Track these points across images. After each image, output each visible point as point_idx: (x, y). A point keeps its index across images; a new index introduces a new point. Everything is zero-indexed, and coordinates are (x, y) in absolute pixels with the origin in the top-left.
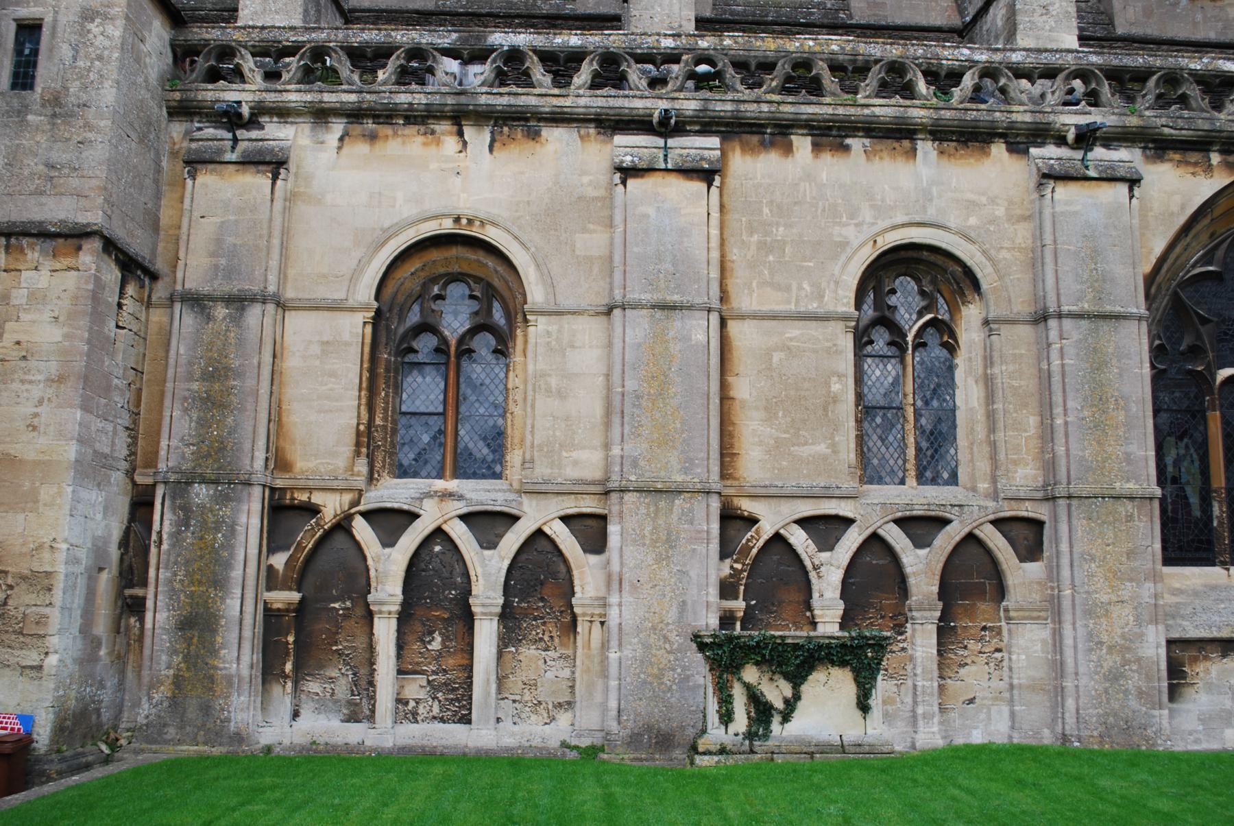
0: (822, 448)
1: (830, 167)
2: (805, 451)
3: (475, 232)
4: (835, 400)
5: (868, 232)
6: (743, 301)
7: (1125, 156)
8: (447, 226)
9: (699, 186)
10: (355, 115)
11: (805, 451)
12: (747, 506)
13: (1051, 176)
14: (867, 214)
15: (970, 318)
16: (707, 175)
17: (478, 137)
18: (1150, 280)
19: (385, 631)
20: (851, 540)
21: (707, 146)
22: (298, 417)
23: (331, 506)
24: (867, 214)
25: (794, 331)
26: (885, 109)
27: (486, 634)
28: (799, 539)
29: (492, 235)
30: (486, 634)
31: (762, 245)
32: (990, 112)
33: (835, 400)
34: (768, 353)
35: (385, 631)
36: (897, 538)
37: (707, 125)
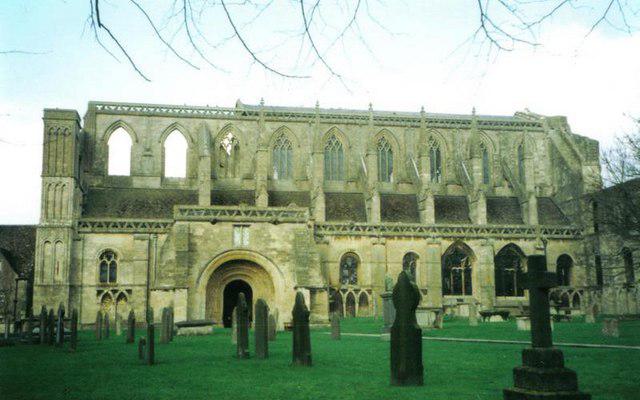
1: (399, 242)
6: (389, 260)
7: (439, 239)
10: (336, 235)
13: (429, 244)
15: (418, 262)
16: (384, 244)
17: (353, 238)
18: (442, 257)
19: (344, 305)
21: (383, 240)
22: (332, 277)
23: (336, 289)
26: (407, 233)
27: (357, 305)
30: (357, 305)
32: (420, 234)
35: (344, 305)
37: (384, 236)
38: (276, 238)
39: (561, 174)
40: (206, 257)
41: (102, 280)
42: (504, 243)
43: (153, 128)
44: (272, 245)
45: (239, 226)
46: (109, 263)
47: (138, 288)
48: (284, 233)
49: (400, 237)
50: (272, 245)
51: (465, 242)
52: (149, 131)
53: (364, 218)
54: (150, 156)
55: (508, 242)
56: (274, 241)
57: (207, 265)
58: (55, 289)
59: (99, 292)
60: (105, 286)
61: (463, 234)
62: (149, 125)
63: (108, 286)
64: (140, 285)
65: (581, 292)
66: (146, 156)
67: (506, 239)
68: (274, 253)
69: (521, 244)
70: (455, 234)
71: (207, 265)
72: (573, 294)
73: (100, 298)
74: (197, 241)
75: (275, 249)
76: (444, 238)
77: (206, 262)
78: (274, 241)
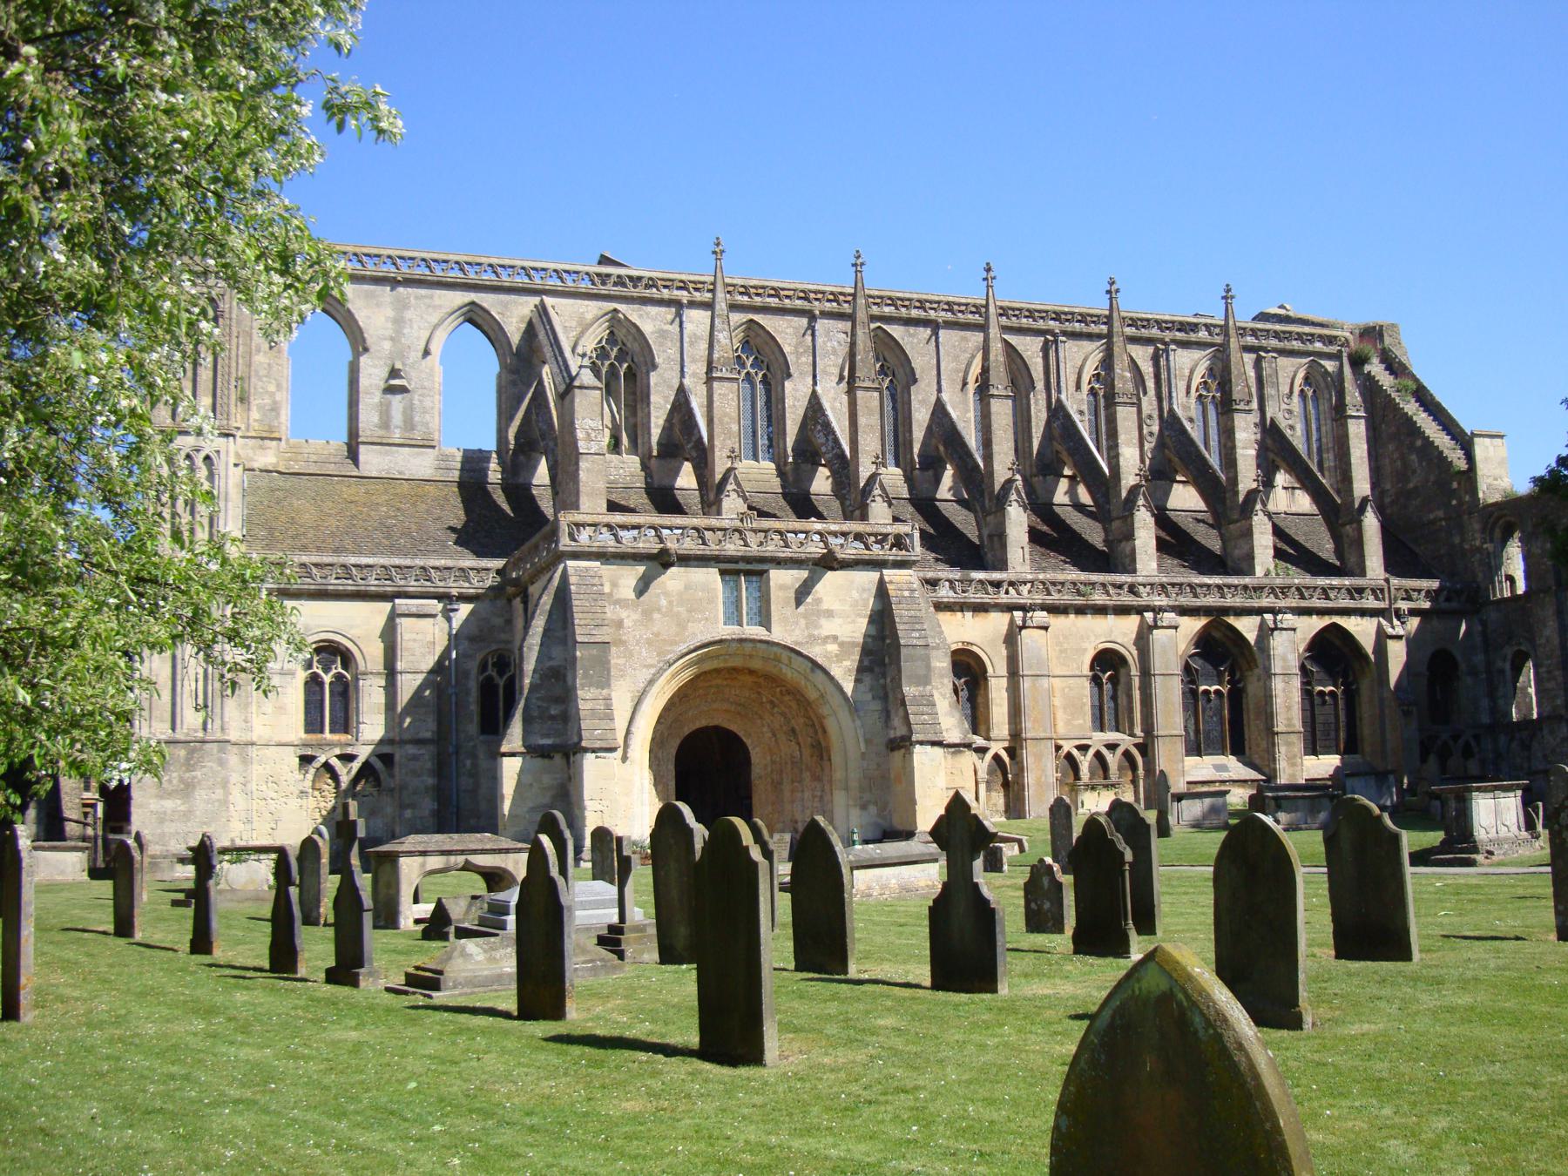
0: (1081, 722)
2: (1076, 722)
3: (969, 648)
4: (1084, 704)
5: (1093, 645)
8: (960, 646)
9: (1043, 632)
11: (1076, 722)
12: (1061, 742)
14: (1093, 638)
17: (969, 615)
20: (1091, 752)
24: (1093, 638)
25: (1071, 681)
28: (1075, 752)
29: (974, 649)
31: (1061, 651)
33: (1084, 704)
34: (1063, 689)
36: (1105, 751)
37: (1044, 607)
38: (836, 606)
39: (1403, 458)
40: (654, 662)
41: (313, 723)
42: (1317, 623)
43: (409, 314)
44: (828, 627)
45: (737, 573)
46: (327, 679)
47: (411, 750)
48: (855, 595)
49: (1080, 611)
50: (828, 627)
51: (1231, 620)
52: (399, 322)
53: (1002, 565)
54: (403, 390)
55: (1326, 621)
56: (830, 614)
57: (651, 682)
58: (191, 752)
59: (306, 760)
60: (321, 745)
61: (1230, 601)
62: (402, 306)
63: (331, 745)
64: (419, 742)
65: (1476, 737)
66: (390, 390)
67: (1322, 612)
68: (833, 648)
69: (1351, 624)
70: (1211, 600)
71: (651, 682)
72: (1461, 742)
73: (310, 776)
74: (624, 614)
75: (835, 638)
76: (1184, 611)
77: (647, 674)
78: (830, 614)
